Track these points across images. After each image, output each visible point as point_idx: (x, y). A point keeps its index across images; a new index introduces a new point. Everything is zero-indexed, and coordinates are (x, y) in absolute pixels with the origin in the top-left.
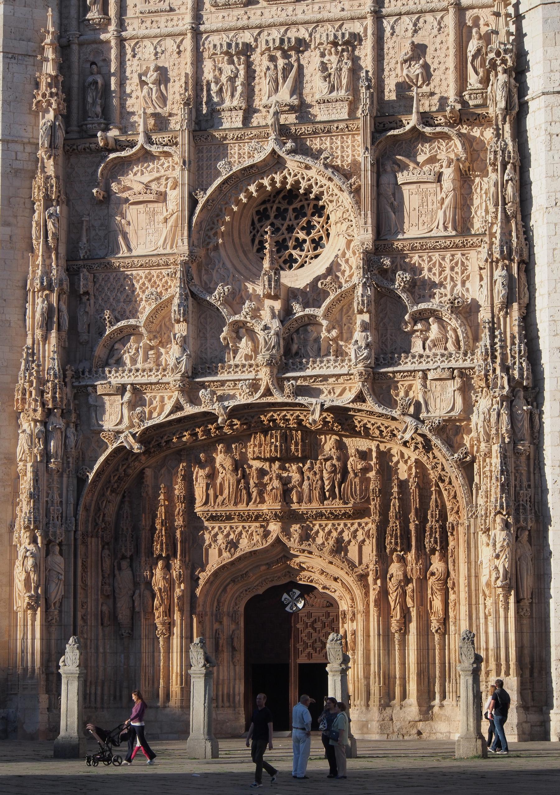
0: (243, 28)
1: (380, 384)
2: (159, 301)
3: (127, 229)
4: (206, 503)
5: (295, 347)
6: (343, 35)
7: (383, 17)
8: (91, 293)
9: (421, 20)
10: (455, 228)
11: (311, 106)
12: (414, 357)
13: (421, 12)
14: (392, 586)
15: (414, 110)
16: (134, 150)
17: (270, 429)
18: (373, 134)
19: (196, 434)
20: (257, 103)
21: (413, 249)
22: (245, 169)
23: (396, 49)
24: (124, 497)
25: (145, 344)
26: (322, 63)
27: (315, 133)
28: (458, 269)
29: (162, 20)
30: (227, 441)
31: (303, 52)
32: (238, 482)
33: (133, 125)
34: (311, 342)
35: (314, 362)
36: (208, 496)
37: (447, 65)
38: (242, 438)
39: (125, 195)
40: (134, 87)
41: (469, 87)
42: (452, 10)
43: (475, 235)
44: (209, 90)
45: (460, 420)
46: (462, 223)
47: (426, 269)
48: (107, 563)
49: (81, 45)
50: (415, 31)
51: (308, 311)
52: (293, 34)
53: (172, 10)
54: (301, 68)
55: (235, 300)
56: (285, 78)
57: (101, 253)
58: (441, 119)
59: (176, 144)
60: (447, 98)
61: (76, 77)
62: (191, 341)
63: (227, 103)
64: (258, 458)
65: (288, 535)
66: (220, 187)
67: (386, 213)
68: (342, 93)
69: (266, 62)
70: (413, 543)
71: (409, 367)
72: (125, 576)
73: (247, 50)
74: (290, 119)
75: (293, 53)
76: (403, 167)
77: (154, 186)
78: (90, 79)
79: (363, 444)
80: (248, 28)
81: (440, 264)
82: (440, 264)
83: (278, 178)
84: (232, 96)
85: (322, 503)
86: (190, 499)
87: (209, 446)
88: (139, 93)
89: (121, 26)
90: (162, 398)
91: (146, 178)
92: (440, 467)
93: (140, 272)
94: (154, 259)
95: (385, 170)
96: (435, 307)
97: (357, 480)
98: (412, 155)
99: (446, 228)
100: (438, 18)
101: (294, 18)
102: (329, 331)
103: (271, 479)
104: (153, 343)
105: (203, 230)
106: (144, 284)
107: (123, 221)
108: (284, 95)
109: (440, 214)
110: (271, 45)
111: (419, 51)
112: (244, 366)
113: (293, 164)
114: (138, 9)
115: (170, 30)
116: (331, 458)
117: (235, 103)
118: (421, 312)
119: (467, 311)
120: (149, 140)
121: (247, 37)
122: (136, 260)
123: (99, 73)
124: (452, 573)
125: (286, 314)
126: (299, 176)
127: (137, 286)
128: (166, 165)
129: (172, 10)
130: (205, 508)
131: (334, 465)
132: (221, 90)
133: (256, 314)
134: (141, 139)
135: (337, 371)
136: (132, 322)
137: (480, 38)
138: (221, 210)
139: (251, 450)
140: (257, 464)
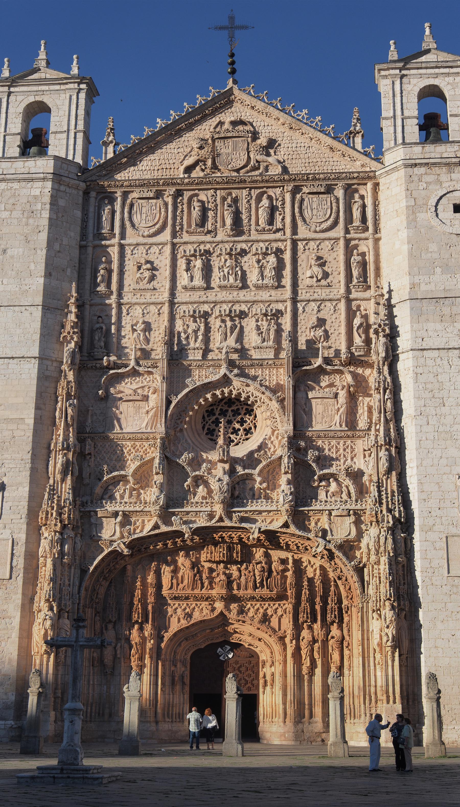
0: (204, 303)
1: (299, 517)
2: (143, 461)
3: (120, 416)
4: (171, 588)
5: (237, 493)
6: (272, 310)
7: (298, 302)
8: (93, 454)
9: (323, 305)
10: (347, 426)
11: (248, 350)
12: (321, 502)
13: (323, 300)
14: (303, 644)
15: (320, 355)
16: (127, 369)
17: (219, 542)
18: (293, 367)
19: (166, 545)
20: (211, 346)
21: (319, 437)
22: (205, 384)
23: (306, 320)
24: (111, 582)
25: (131, 487)
26: (257, 325)
27: (252, 365)
28: (349, 450)
29: (148, 295)
30: (187, 549)
31: (243, 318)
32: (195, 575)
33: (126, 355)
34: (248, 490)
35: (252, 502)
36: (172, 583)
37: (340, 331)
38: (199, 548)
39: (119, 396)
40: (127, 333)
41: (355, 345)
42: (343, 301)
43: (360, 430)
44: (179, 337)
45: (353, 542)
46: (351, 423)
47: (327, 449)
48: (98, 626)
49: (91, 305)
50: (319, 311)
51: (247, 471)
52: (237, 308)
53: (155, 289)
54: (242, 328)
55: (196, 463)
56: (232, 333)
57: (101, 430)
58: (337, 362)
59: (157, 367)
60: (340, 350)
61: (87, 324)
62: (165, 486)
63: (192, 345)
64: (210, 561)
65: (230, 611)
66: (187, 395)
67: (301, 414)
68: (271, 343)
69: (218, 323)
70: (319, 618)
71: (318, 507)
72: (110, 635)
73: (206, 315)
74: (235, 356)
75: (237, 319)
76: (313, 389)
77: (139, 391)
78: (98, 326)
79: (283, 554)
80: (207, 302)
81: (336, 447)
82: (336, 447)
83: (226, 391)
84: (196, 341)
85: (255, 590)
86: (159, 586)
87: (175, 551)
88: (130, 335)
89: (120, 296)
90: (143, 521)
91: (134, 386)
92: (339, 570)
93: (128, 443)
94: (139, 435)
95: (299, 390)
96: (335, 472)
97: (279, 577)
98: (318, 383)
99: (341, 426)
100: (334, 304)
101: (239, 299)
102: (261, 484)
103: (218, 575)
104: (136, 487)
105: (175, 420)
106: (130, 450)
107: (117, 411)
108: (231, 342)
109: (337, 418)
110: (223, 313)
111: (321, 322)
112: (202, 503)
113: (237, 383)
114: (132, 286)
115: (153, 300)
116: (261, 562)
117: (197, 345)
118: (324, 475)
119: (356, 476)
120: (138, 364)
121: (206, 308)
122: (126, 435)
123: (102, 323)
124: (347, 638)
125: (232, 472)
126: (241, 390)
127: (125, 451)
128: (148, 379)
129: (155, 289)
130: (171, 592)
131: (263, 567)
132: (188, 337)
133: (209, 471)
134: (132, 363)
135: (269, 508)
136: (122, 473)
137: (362, 317)
138: (186, 408)
139: (204, 556)
140: (207, 565)
